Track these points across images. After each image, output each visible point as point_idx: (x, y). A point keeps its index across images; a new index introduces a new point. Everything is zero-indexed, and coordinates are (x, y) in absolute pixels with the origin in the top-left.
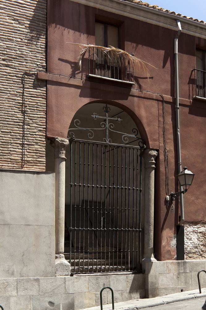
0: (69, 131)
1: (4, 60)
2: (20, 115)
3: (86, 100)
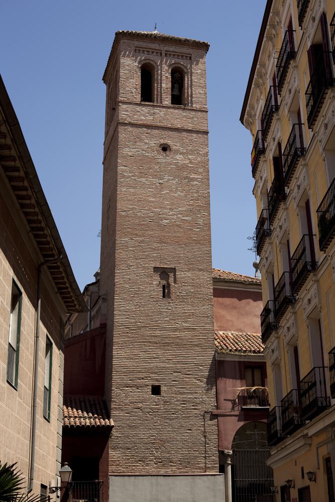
0: (232, 445)
1: (193, 406)
2: (203, 439)
3: (242, 423)
